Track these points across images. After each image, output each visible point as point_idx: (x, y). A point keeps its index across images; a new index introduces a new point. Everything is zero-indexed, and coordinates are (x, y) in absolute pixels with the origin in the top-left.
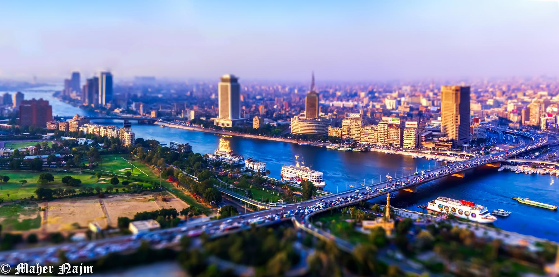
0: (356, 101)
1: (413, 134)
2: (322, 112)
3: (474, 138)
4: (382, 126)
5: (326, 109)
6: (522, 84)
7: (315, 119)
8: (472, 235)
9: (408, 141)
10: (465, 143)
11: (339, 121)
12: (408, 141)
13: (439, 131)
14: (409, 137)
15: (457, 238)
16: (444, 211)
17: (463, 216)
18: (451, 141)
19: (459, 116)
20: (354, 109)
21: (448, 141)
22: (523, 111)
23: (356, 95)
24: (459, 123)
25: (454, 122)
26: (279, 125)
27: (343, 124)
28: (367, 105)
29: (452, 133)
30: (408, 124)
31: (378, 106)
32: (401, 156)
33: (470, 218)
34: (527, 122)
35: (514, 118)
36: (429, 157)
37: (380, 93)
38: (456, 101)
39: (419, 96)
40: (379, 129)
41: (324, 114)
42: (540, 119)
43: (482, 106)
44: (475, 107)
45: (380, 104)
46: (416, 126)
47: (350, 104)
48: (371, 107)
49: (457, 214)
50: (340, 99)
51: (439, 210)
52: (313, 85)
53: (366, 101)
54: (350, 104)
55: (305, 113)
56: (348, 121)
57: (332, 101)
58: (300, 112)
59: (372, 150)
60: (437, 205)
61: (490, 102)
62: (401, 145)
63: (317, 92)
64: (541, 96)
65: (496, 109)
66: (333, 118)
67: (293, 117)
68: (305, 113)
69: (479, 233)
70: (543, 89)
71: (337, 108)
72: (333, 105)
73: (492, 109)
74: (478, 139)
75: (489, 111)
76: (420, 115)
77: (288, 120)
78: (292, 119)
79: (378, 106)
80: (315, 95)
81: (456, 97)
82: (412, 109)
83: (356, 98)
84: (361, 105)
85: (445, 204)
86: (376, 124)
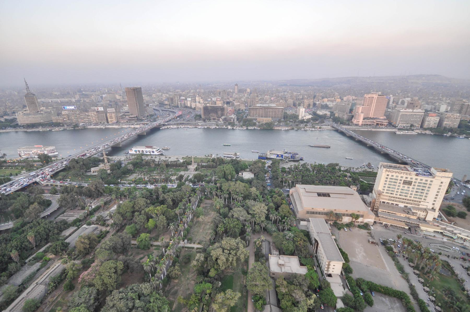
1: (113, 115)
4: (92, 112)
7: (38, 112)
8: (154, 161)
9: (111, 120)
11: (60, 112)
12: (111, 120)
13: (129, 113)
14: (111, 117)
15: (148, 163)
16: (138, 153)
17: (148, 153)
21: (134, 117)
26: (6, 120)
30: (109, 110)
31: (87, 100)
32: (109, 129)
33: (152, 153)
40: (90, 114)
46: (114, 111)
49: (145, 153)
51: (135, 153)
55: (27, 109)
58: (24, 108)
59: (89, 127)
60: (134, 150)
62: (108, 122)
64: (177, 92)
68: (27, 109)
69: (157, 160)
72: (52, 101)
76: (116, 104)
77: (14, 114)
85: (138, 149)
86: (87, 111)
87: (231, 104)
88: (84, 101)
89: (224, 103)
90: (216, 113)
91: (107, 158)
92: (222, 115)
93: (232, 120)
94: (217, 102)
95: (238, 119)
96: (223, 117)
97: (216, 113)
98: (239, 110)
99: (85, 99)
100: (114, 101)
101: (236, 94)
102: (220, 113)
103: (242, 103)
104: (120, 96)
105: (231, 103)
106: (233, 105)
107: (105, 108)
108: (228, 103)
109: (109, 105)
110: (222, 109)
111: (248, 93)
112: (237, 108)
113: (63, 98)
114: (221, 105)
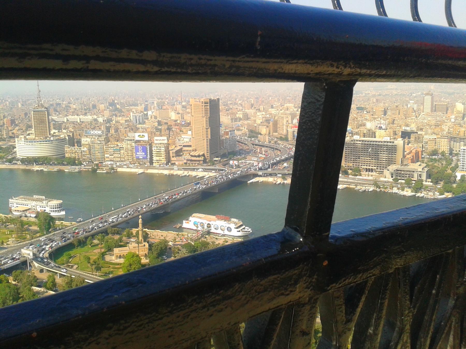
0: (95, 114)
2: (55, 128)
3: (225, 151)
5: (59, 127)
6: (269, 96)
10: (217, 157)
18: (202, 156)
19: (209, 130)
20: (94, 125)
22: (271, 124)
23: (94, 106)
24: (209, 137)
25: (205, 136)
27: (83, 142)
28: (109, 121)
29: (203, 148)
31: (122, 120)
34: (276, 134)
35: (264, 130)
36: (180, 173)
37: (122, 104)
38: (206, 114)
39: (168, 109)
41: (57, 131)
42: (287, 131)
43: (232, 119)
44: (224, 119)
45: (124, 119)
47: (89, 118)
48: (114, 122)
50: (75, 113)
52: (39, 97)
53: (107, 114)
54: (89, 118)
56: (89, 140)
57: (66, 116)
58: (27, 130)
61: (240, 115)
63: (46, 105)
65: (246, 122)
66: (68, 136)
67: (18, 137)
70: (289, 102)
71: (73, 123)
72: (67, 120)
73: (241, 121)
74: (229, 153)
75: (240, 123)
77: (12, 140)
78: (16, 139)
79: (122, 120)
80: (43, 109)
81: (206, 110)
82: (159, 123)
83: (95, 111)
84: (101, 120)
87: (412, 139)
88: (117, 122)
89: (395, 133)
90: (375, 155)
91: (143, 232)
92: (391, 162)
93: (416, 175)
94: (378, 132)
95: (429, 176)
96: (393, 168)
97: (375, 155)
98: (435, 153)
99: (120, 118)
100: (166, 123)
101: (427, 114)
102: (384, 156)
103: (443, 137)
104: (179, 114)
105: (413, 136)
106: (419, 139)
107: (152, 135)
108: (405, 135)
109: (157, 129)
110: (392, 149)
111: (459, 112)
112: (430, 147)
113: (85, 114)
114: (388, 139)
